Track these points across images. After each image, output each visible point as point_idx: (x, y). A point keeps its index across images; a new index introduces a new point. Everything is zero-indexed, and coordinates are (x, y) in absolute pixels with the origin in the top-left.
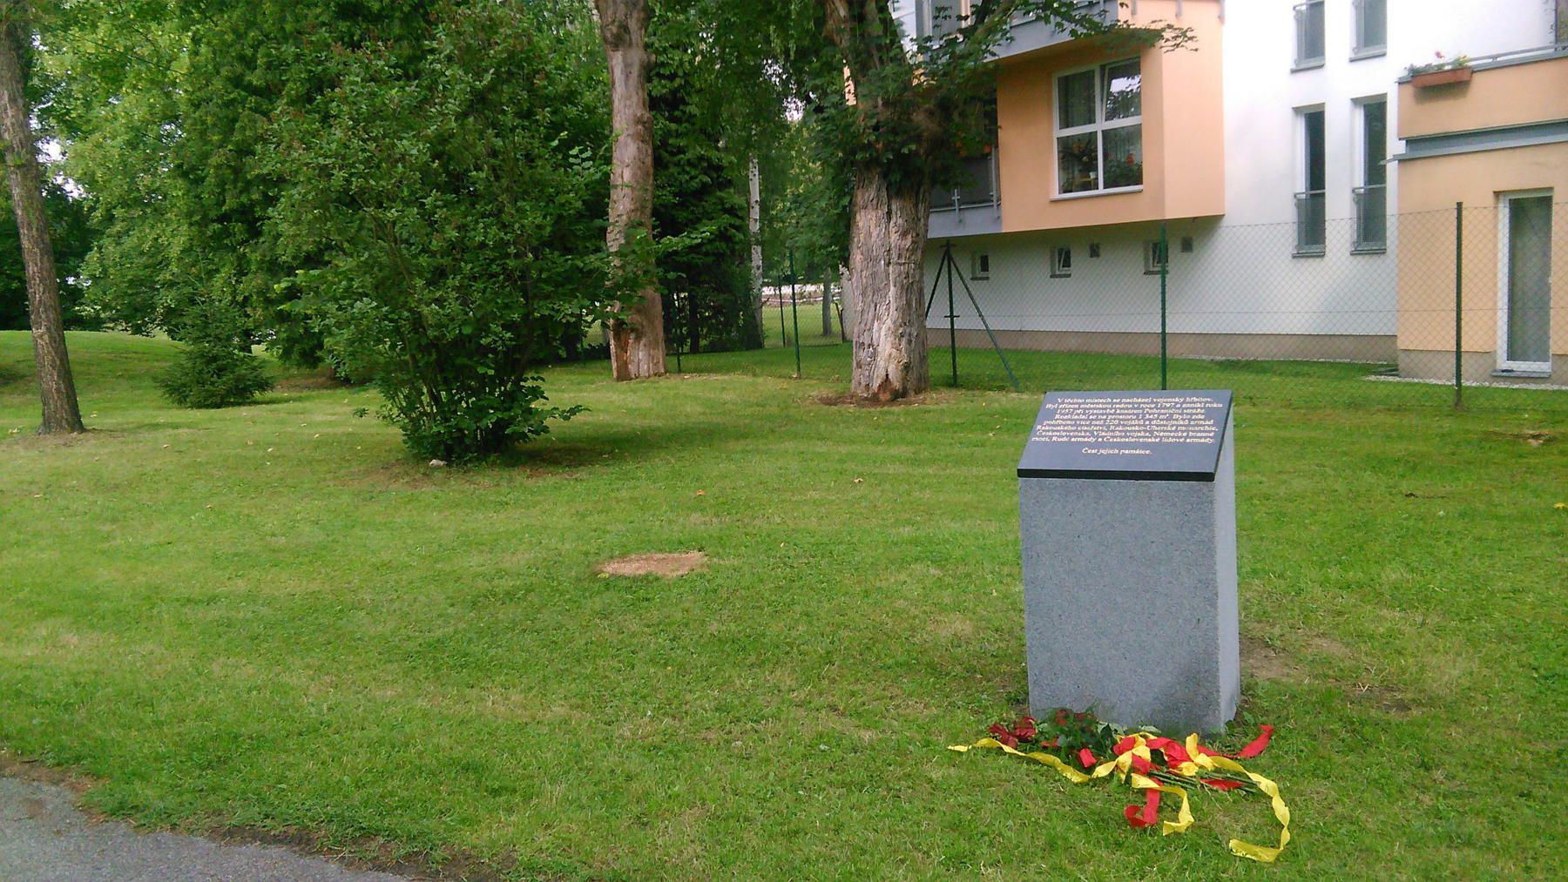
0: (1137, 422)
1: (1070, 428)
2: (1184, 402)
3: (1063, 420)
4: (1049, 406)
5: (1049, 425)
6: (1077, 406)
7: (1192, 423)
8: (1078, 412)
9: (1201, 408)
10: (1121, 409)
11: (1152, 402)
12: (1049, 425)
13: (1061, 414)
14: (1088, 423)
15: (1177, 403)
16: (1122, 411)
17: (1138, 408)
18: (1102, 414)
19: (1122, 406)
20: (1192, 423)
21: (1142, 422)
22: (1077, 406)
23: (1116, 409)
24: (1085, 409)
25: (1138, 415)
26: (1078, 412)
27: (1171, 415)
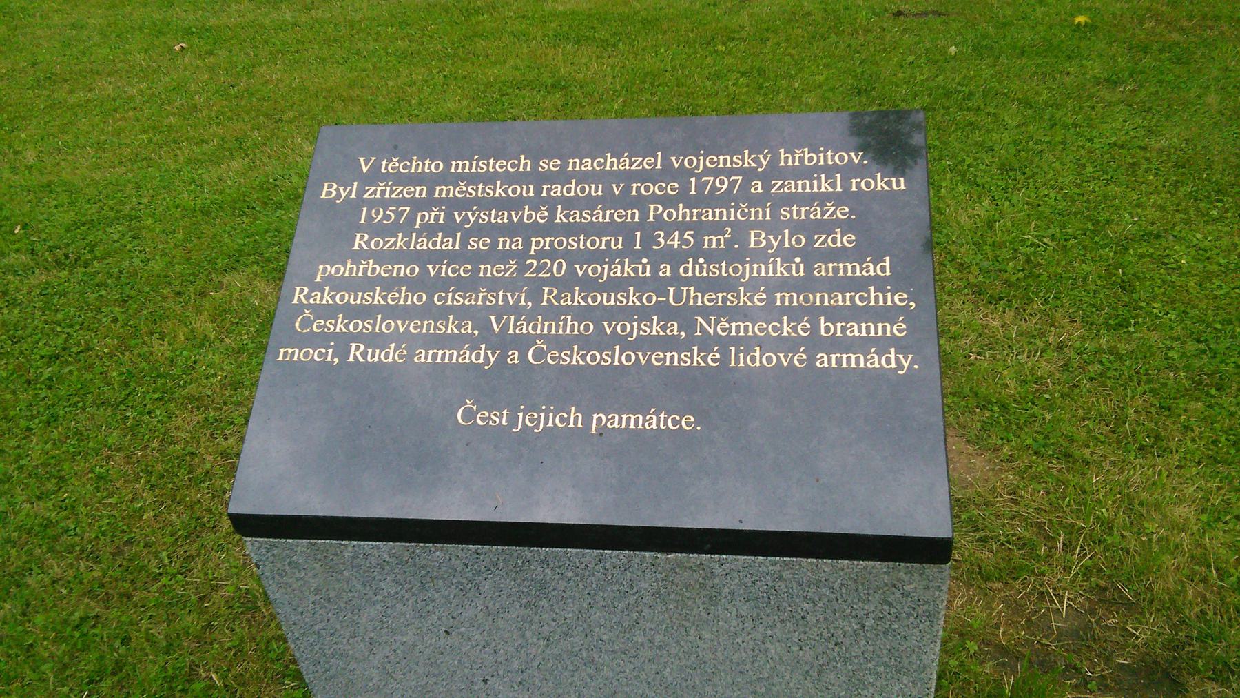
0: (625, 269)
1: (404, 297)
2: (774, 172)
3: (381, 257)
4: (330, 190)
5: (338, 284)
6: (420, 192)
7: (823, 270)
8: (430, 217)
9: (839, 200)
10: (569, 203)
11: (668, 173)
12: (338, 284)
13: (379, 231)
14: (464, 271)
15: (749, 174)
16: (576, 217)
17: (626, 201)
18: (511, 230)
19: (573, 190)
20: (823, 270)
21: (645, 269)
22: (420, 192)
23: (551, 203)
24: (453, 205)
25: (625, 230)
26: (430, 217)
27: (740, 229)
